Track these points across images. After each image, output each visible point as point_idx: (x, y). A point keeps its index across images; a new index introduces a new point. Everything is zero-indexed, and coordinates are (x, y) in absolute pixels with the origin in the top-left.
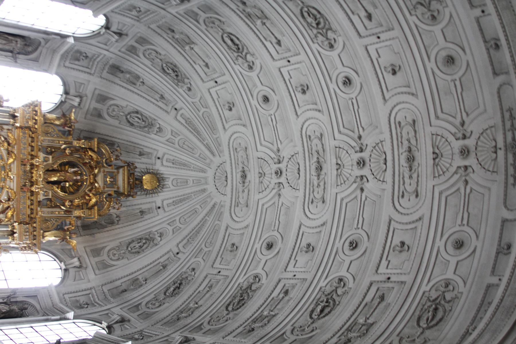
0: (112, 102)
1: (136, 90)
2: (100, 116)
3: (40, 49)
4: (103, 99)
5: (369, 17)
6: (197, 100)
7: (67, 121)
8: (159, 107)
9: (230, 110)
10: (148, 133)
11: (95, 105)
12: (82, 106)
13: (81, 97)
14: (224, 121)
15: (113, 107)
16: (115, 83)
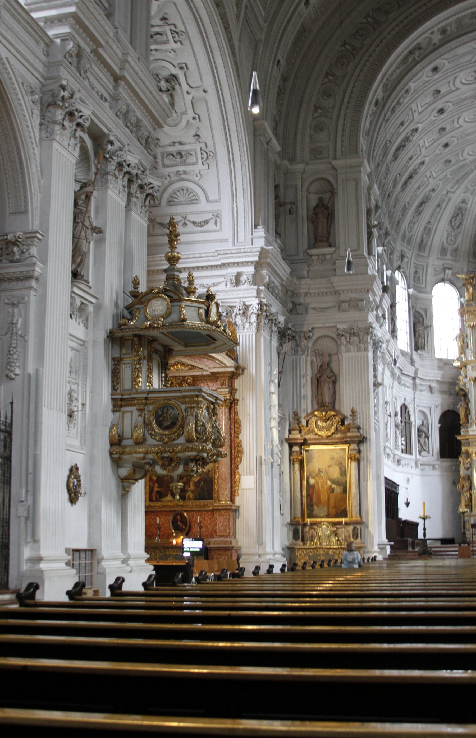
0: (445, 243)
1: (435, 227)
2: (456, 250)
3: (418, 310)
4: (443, 251)
5: (402, 124)
6: (441, 183)
7: (468, 283)
8: (446, 206)
9: (450, 161)
10: (466, 210)
11: (448, 257)
12: (450, 266)
13: (445, 269)
14: (458, 161)
15: (449, 241)
16: (431, 244)
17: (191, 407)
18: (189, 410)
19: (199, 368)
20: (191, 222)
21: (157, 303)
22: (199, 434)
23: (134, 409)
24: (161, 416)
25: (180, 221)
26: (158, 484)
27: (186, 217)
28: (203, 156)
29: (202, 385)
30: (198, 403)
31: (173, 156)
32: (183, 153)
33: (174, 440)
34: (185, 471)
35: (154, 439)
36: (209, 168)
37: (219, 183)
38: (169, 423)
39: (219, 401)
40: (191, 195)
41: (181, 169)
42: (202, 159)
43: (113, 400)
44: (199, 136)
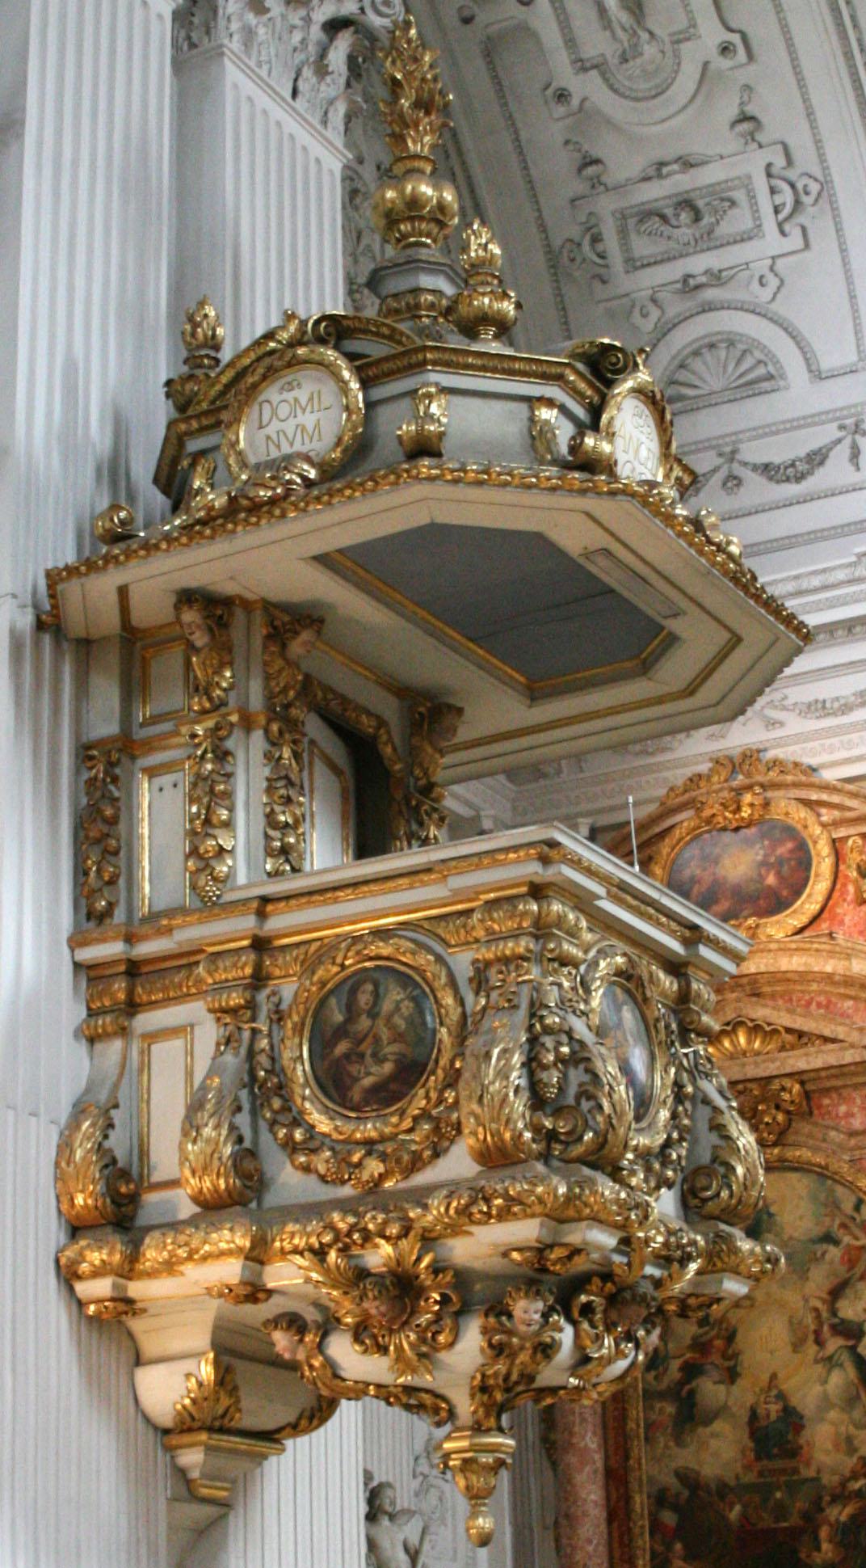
17: (505, 960)
18: (495, 978)
19: (826, 1040)
20: (755, 468)
21: (289, 396)
22: (558, 1112)
23: (194, 1011)
24: (341, 1032)
25: (715, 471)
26: (686, 1547)
27: (734, 452)
28: (778, 200)
29: (843, 1109)
30: (542, 930)
31: (664, 218)
32: (700, 203)
33: (416, 1164)
34: (498, 1350)
35: (307, 1169)
36: (807, 246)
37: (852, 297)
38: (388, 1067)
39: (705, 951)
40: (748, 362)
41: (699, 264)
42: (777, 210)
43: (90, 974)
44: (752, 118)
